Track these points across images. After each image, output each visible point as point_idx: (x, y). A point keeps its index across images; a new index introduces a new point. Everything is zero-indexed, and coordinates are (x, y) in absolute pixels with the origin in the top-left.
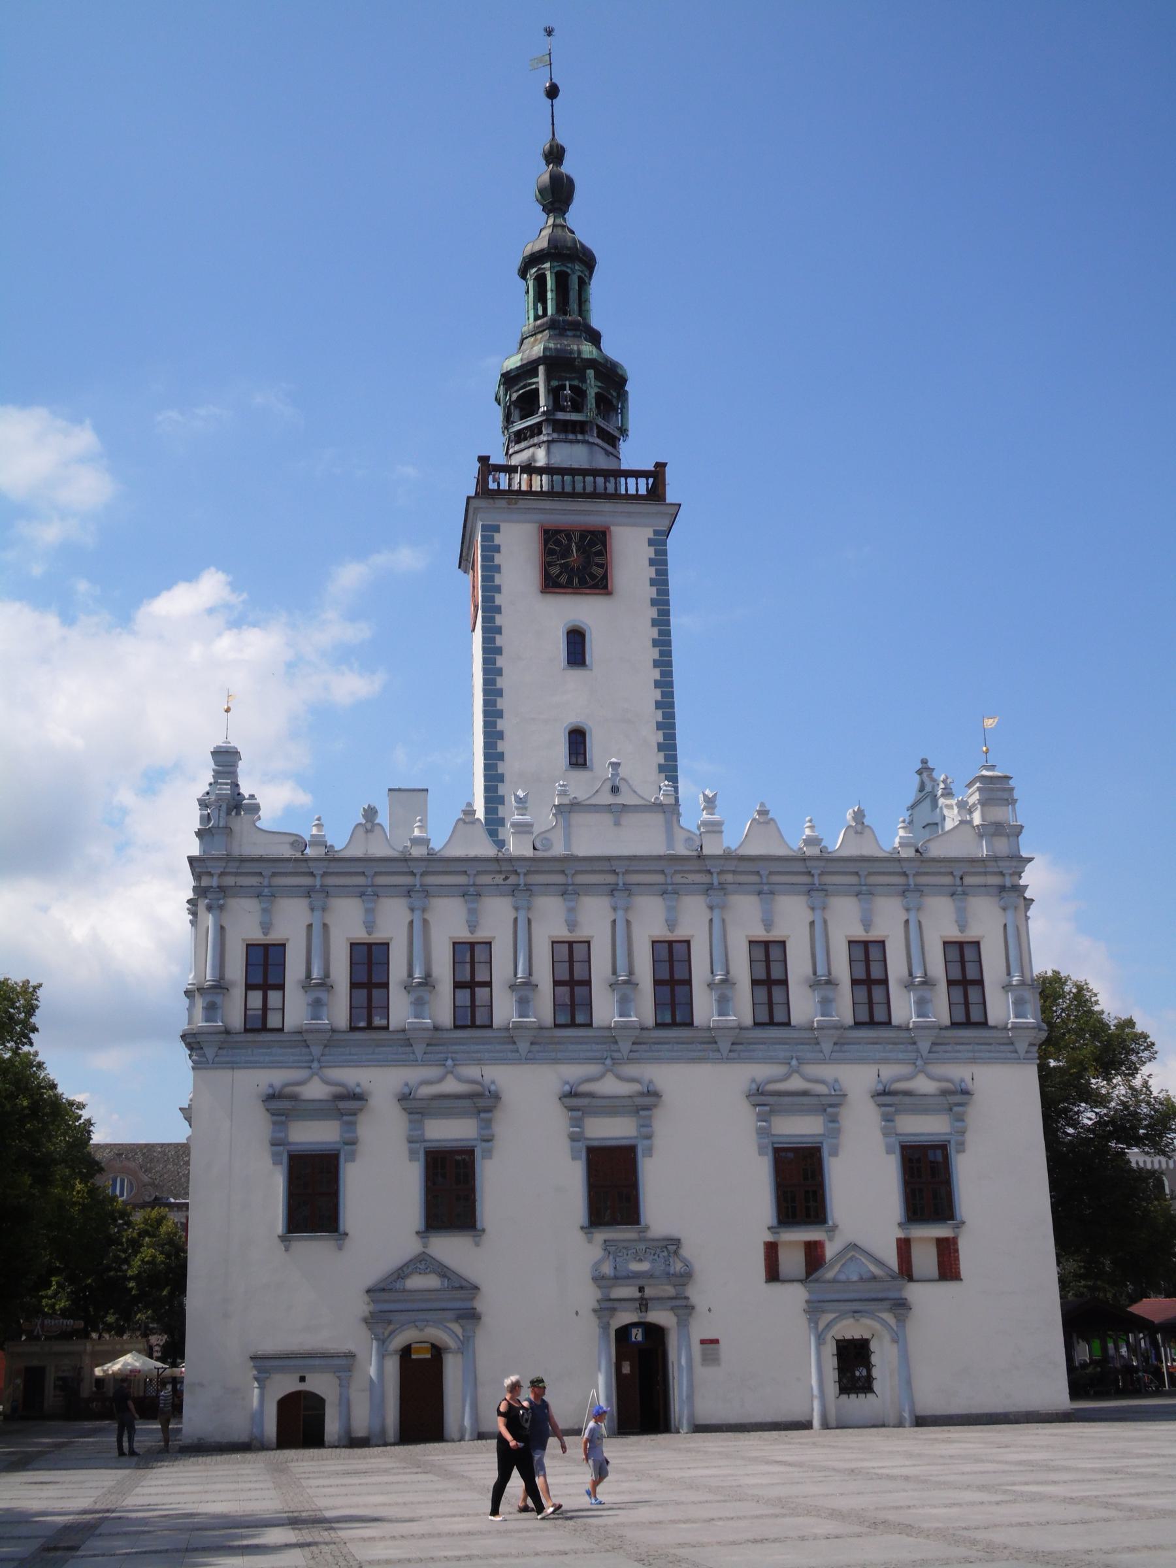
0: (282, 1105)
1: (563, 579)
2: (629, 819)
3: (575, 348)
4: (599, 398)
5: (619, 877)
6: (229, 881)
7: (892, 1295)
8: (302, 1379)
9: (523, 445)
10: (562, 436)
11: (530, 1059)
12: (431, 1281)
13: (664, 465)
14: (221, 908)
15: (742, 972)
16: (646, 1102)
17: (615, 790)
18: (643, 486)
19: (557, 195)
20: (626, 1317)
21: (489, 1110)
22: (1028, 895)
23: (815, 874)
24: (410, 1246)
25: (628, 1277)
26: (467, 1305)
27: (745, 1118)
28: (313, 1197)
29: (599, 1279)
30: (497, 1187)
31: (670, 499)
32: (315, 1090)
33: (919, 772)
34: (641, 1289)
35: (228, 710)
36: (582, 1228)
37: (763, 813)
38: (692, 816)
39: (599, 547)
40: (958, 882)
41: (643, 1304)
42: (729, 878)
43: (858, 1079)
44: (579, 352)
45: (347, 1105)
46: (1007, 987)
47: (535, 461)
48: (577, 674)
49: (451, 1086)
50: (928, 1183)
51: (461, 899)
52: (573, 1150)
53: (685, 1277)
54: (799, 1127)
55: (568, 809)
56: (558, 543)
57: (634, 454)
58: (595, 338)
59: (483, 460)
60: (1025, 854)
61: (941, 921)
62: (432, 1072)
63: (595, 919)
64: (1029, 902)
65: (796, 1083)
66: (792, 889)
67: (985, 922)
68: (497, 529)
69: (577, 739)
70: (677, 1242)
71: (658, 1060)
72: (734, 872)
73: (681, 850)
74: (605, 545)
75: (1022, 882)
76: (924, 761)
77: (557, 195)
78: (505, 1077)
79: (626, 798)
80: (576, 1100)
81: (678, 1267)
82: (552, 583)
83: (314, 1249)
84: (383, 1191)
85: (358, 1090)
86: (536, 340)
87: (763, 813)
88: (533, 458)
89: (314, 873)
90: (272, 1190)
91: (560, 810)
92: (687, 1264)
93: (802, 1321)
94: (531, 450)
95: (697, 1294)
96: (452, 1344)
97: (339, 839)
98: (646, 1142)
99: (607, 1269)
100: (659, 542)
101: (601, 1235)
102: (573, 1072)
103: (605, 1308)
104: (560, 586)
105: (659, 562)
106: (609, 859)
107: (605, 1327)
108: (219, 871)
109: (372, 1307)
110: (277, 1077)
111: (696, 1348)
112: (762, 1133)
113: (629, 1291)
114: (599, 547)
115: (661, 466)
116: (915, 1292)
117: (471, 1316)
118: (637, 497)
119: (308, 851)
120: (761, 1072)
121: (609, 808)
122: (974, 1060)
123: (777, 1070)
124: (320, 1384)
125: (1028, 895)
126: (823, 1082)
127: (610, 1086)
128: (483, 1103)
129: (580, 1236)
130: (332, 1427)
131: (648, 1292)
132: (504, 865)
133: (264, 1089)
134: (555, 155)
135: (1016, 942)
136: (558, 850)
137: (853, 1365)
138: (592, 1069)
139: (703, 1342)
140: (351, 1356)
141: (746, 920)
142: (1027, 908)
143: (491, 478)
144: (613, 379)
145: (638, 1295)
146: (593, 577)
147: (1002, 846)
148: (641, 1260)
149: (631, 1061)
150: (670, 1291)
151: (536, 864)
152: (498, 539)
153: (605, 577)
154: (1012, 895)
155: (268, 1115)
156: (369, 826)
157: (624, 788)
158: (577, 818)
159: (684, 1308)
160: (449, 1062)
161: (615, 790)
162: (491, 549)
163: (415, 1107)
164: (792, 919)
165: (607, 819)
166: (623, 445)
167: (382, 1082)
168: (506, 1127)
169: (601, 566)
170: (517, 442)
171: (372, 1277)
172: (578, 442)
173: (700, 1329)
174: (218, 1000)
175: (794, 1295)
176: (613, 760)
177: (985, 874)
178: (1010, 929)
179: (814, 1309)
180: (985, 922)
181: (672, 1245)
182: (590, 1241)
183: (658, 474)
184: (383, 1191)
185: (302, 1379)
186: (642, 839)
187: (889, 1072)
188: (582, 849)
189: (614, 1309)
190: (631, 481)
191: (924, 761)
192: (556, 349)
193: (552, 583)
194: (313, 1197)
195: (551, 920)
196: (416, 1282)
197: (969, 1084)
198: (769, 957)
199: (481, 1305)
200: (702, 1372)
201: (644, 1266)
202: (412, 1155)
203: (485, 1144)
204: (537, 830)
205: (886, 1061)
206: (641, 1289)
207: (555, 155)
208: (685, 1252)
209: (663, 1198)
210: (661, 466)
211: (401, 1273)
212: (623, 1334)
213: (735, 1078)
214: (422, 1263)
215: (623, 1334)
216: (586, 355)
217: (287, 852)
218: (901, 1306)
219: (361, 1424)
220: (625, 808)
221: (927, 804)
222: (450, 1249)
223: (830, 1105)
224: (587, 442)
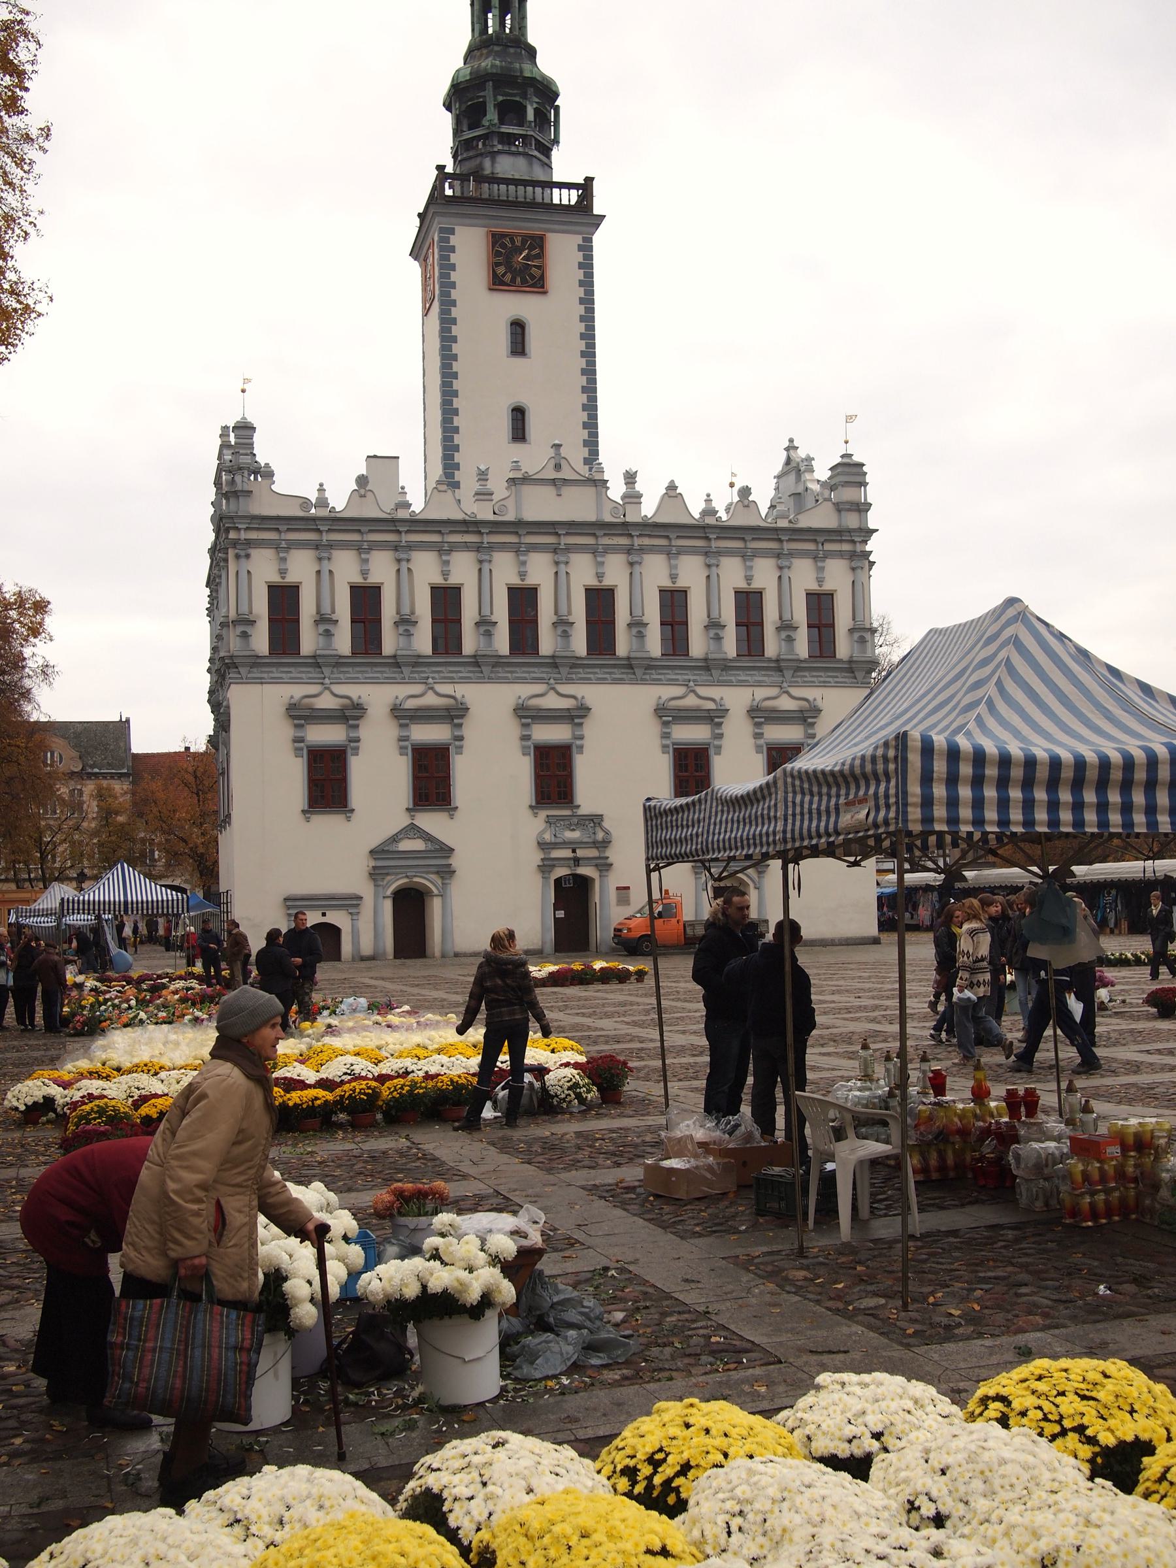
0: (301, 715)
1: (508, 277)
2: (567, 491)
3: (517, 65)
4: (536, 111)
5: (558, 536)
6: (253, 535)
8: (324, 914)
9: (471, 154)
10: (506, 148)
11: (490, 680)
12: (418, 845)
13: (593, 179)
14: (248, 556)
15: (652, 614)
16: (577, 715)
17: (558, 467)
18: (574, 196)
20: (561, 872)
21: (462, 717)
22: (871, 558)
23: (707, 535)
24: (403, 821)
25: (564, 843)
27: (651, 729)
28: (327, 783)
29: (543, 845)
30: (465, 774)
31: (596, 212)
32: (326, 702)
33: (787, 449)
34: (574, 851)
35: (243, 391)
36: (531, 807)
37: (672, 487)
38: (616, 490)
39: (537, 251)
40: (820, 547)
41: (577, 861)
42: (646, 541)
43: (737, 699)
44: (521, 71)
45: (351, 714)
46: (851, 631)
47: (483, 169)
48: (518, 361)
49: (430, 700)
51: (436, 553)
52: (524, 747)
53: (605, 844)
54: (692, 734)
55: (518, 482)
56: (503, 246)
57: (566, 165)
58: (532, 52)
60: (871, 526)
61: (803, 577)
62: (417, 689)
63: (539, 571)
64: (872, 564)
65: (691, 701)
66: (693, 551)
67: (837, 577)
68: (452, 231)
69: (519, 414)
70: (600, 817)
72: (650, 536)
73: (608, 518)
74: (542, 248)
75: (868, 548)
76: (791, 441)
78: (473, 694)
79: (566, 474)
81: (600, 835)
82: (497, 283)
84: (380, 778)
85: (361, 701)
86: (482, 55)
87: (672, 487)
88: (481, 167)
89: (315, 527)
90: (293, 776)
91: (512, 481)
92: (607, 833)
94: (478, 160)
95: (613, 854)
96: (435, 891)
97: (338, 501)
98: (578, 742)
99: (548, 837)
100: (586, 248)
101: (543, 814)
102: (524, 691)
103: (545, 867)
104: (503, 283)
105: (587, 265)
106: (553, 524)
108: (244, 526)
109: (373, 863)
110: (297, 692)
111: (613, 895)
112: (666, 736)
113: (567, 853)
114: (537, 251)
115: (589, 180)
117: (447, 873)
118: (568, 208)
119: (313, 511)
120: (667, 692)
121: (553, 482)
122: (825, 685)
123: (678, 691)
124: (336, 918)
125: (871, 558)
126: (713, 700)
127: (552, 702)
128: (455, 714)
129: (529, 812)
130: (346, 947)
131: (580, 853)
132: (470, 525)
133: (286, 700)
135: (860, 594)
136: (510, 517)
138: (539, 688)
139: (618, 888)
141: (656, 572)
142: (870, 569)
143: (447, 185)
144: (547, 93)
145: (571, 855)
146: (532, 277)
147: (851, 521)
148: (573, 830)
149: (569, 681)
150: (592, 853)
151: (497, 527)
152: (454, 240)
153: (542, 278)
154: (860, 561)
155: (290, 721)
156: (362, 492)
157: (563, 462)
158: (527, 490)
159: (604, 866)
160: (430, 680)
161: (558, 467)
162: (447, 250)
163: (403, 715)
164: (691, 573)
165: (550, 491)
166: (555, 153)
167: (378, 697)
168: (472, 730)
169: (539, 267)
170: (467, 150)
171: (374, 843)
172: (519, 154)
173: (615, 880)
174: (248, 629)
176: (557, 442)
177: (841, 541)
178: (858, 587)
180: (837, 577)
181: (596, 820)
182: (536, 815)
183: (586, 187)
184: (380, 778)
185: (324, 914)
186: (574, 506)
187: (761, 693)
188: (530, 515)
189: (554, 866)
190: (565, 192)
191: (791, 441)
192: (502, 67)
193: (497, 283)
194: (327, 783)
195: (504, 571)
196: (406, 845)
197: (819, 703)
198: (674, 603)
199: (455, 862)
201: (575, 835)
202: (402, 750)
203: (457, 743)
204: (496, 497)
205: (759, 684)
206: (574, 851)
208: (605, 824)
209: (592, 787)
210: (589, 180)
211: (395, 839)
212: (558, 882)
214: (412, 830)
215: (558, 882)
216: (527, 74)
217: (301, 514)
219: (367, 948)
220: (565, 481)
221: (792, 477)
222: (432, 822)
223: (714, 717)
224: (525, 155)
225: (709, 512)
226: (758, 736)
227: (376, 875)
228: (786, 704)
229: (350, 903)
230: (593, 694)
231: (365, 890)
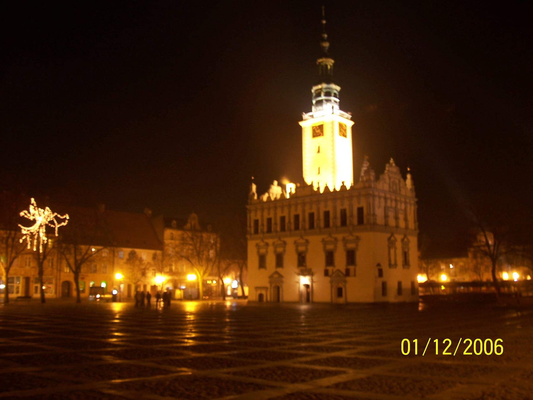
43: (340, 236)
50: (351, 257)
54: (330, 247)
80: (297, 244)
83: (262, 270)
84: (271, 260)
112: (325, 247)
116: (348, 279)
120: (325, 236)
124: (264, 292)
137: (340, 292)
163: (275, 246)
175: (328, 279)
179: (331, 282)
213: (319, 238)
214: (276, 273)
218: (345, 282)
222: (279, 270)
225: (335, 189)
226: (345, 246)
227: (271, 283)
228: (351, 238)
229: (266, 288)
230: (310, 238)
231: (268, 285)
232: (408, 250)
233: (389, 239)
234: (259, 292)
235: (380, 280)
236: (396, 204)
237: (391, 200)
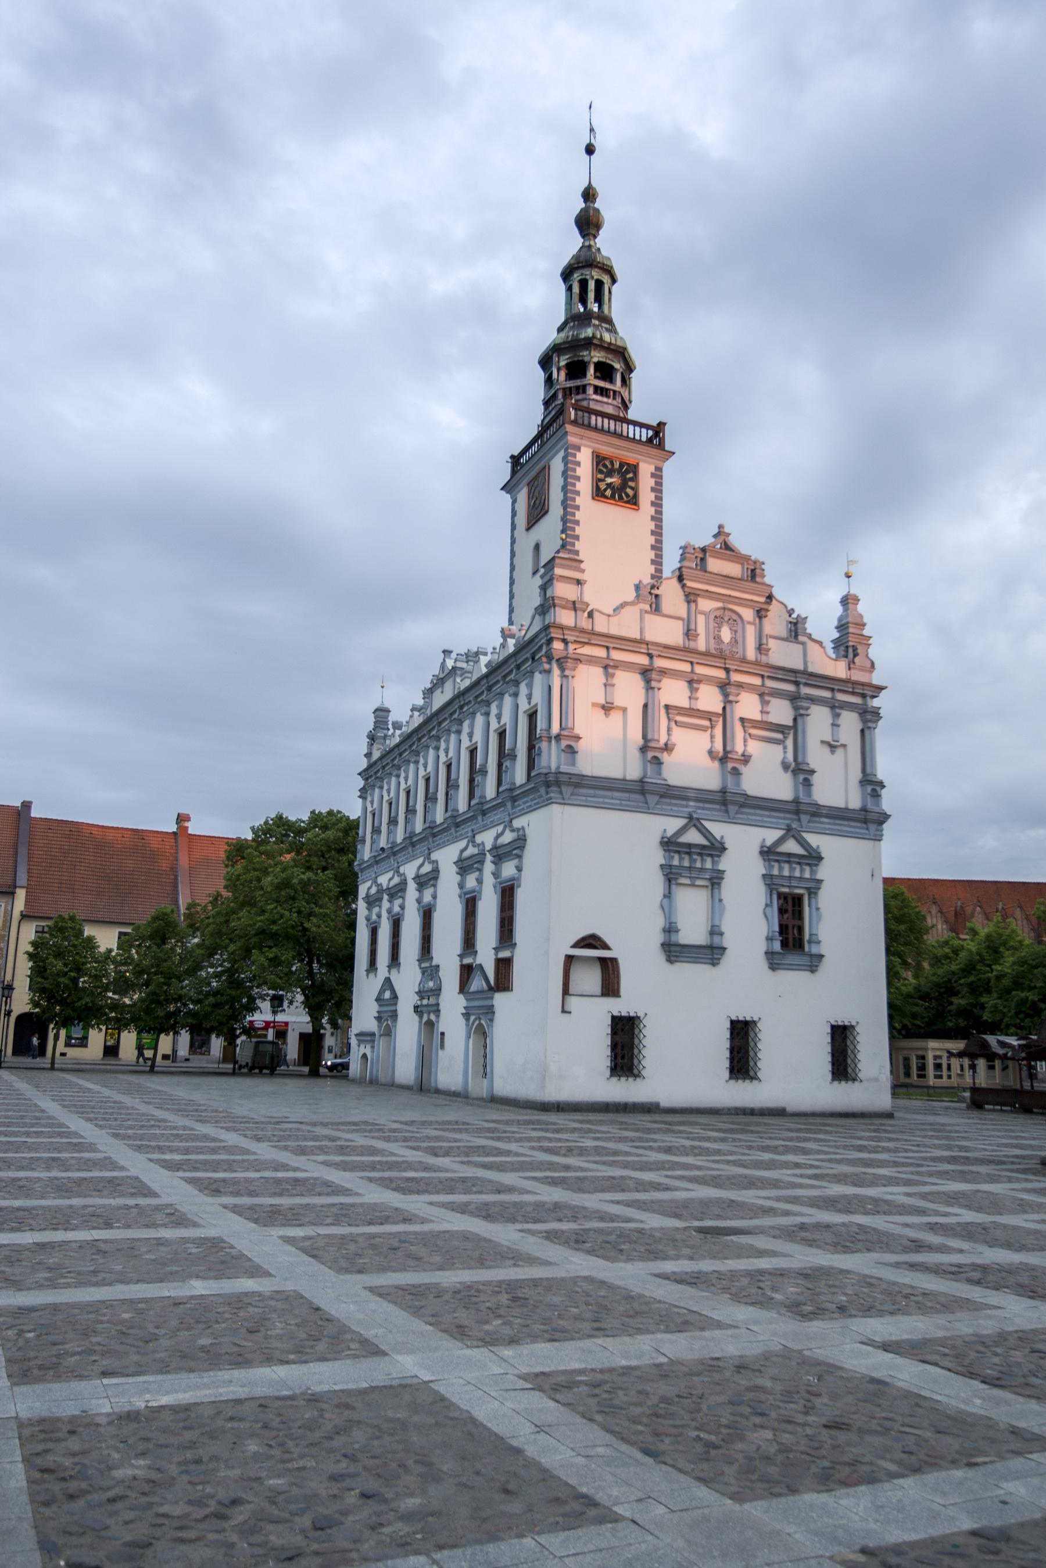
7: (488, 1003)
19: (588, 223)
20: (425, 1018)
26: (392, 1008)
59: (512, 457)
71: (440, 847)
77: (588, 223)
83: (372, 975)
93: (463, 1021)
107: (420, 1022)
112: (461, 886)
116: (500, 1000)
134: (589, 195)
140: (373, 1034)
191: (720, 527)
200: (440, 1052)
207: (589, 195)
232: (814, 887)
233: (668, 844)
234: (362, 1050)
235: (621, 1006)
236: (728, 702)
237: (693, 682)
